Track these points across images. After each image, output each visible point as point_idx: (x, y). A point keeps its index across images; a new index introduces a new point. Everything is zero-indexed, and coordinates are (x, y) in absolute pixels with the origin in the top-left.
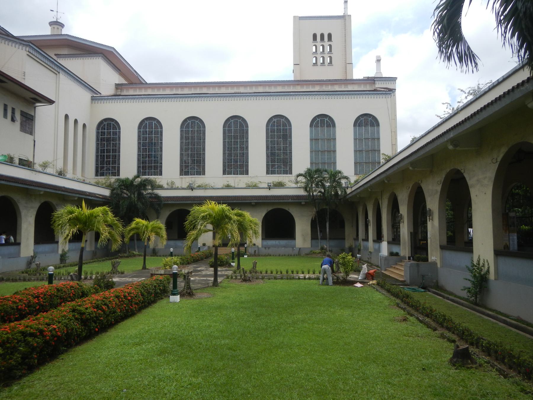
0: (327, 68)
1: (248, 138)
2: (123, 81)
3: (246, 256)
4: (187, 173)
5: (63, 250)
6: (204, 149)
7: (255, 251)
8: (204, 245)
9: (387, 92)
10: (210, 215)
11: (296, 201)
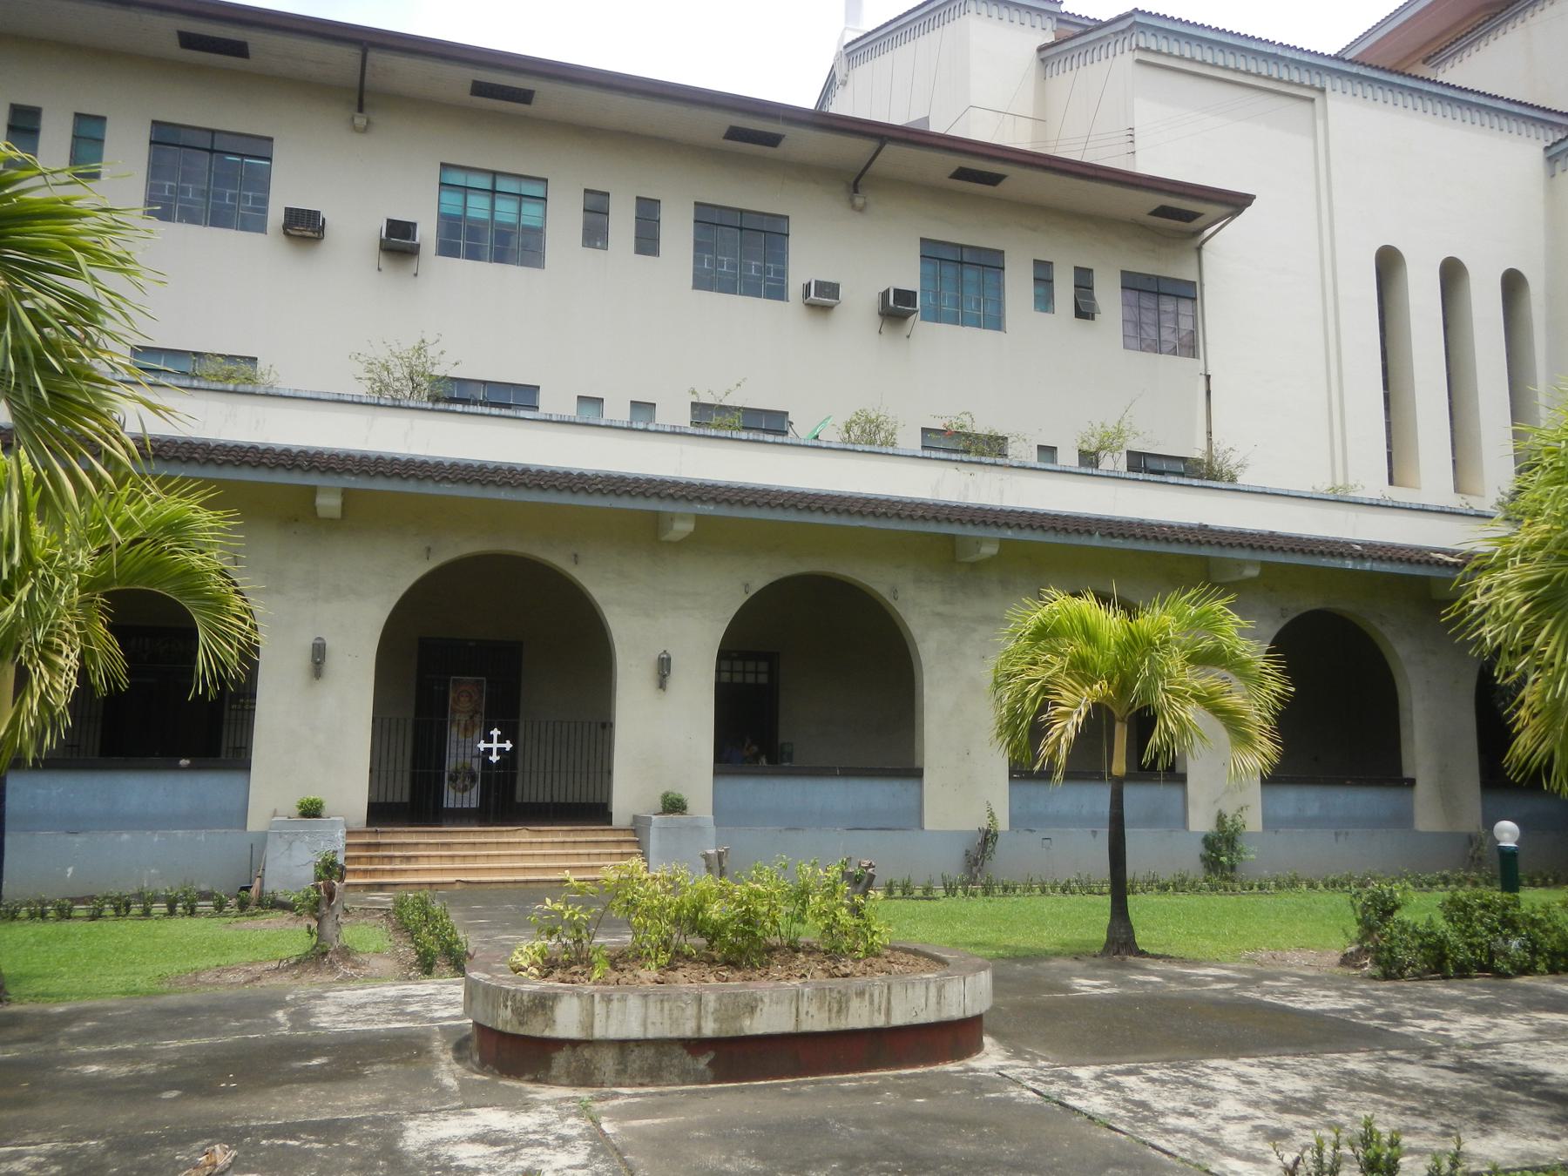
5: (1221, 819)
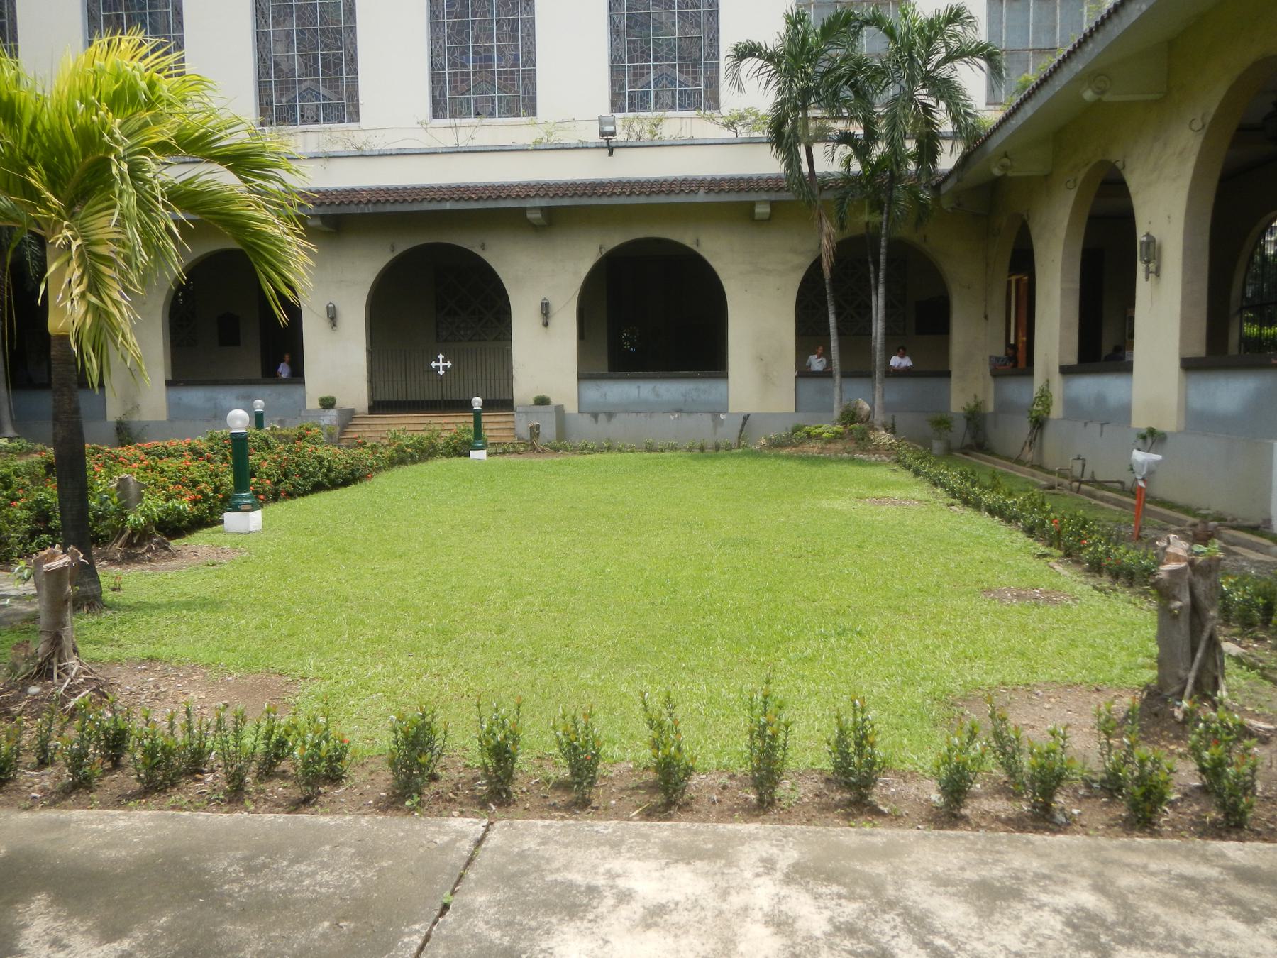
3: (478, 455)
7: (535, 431)
8: (328, 403)
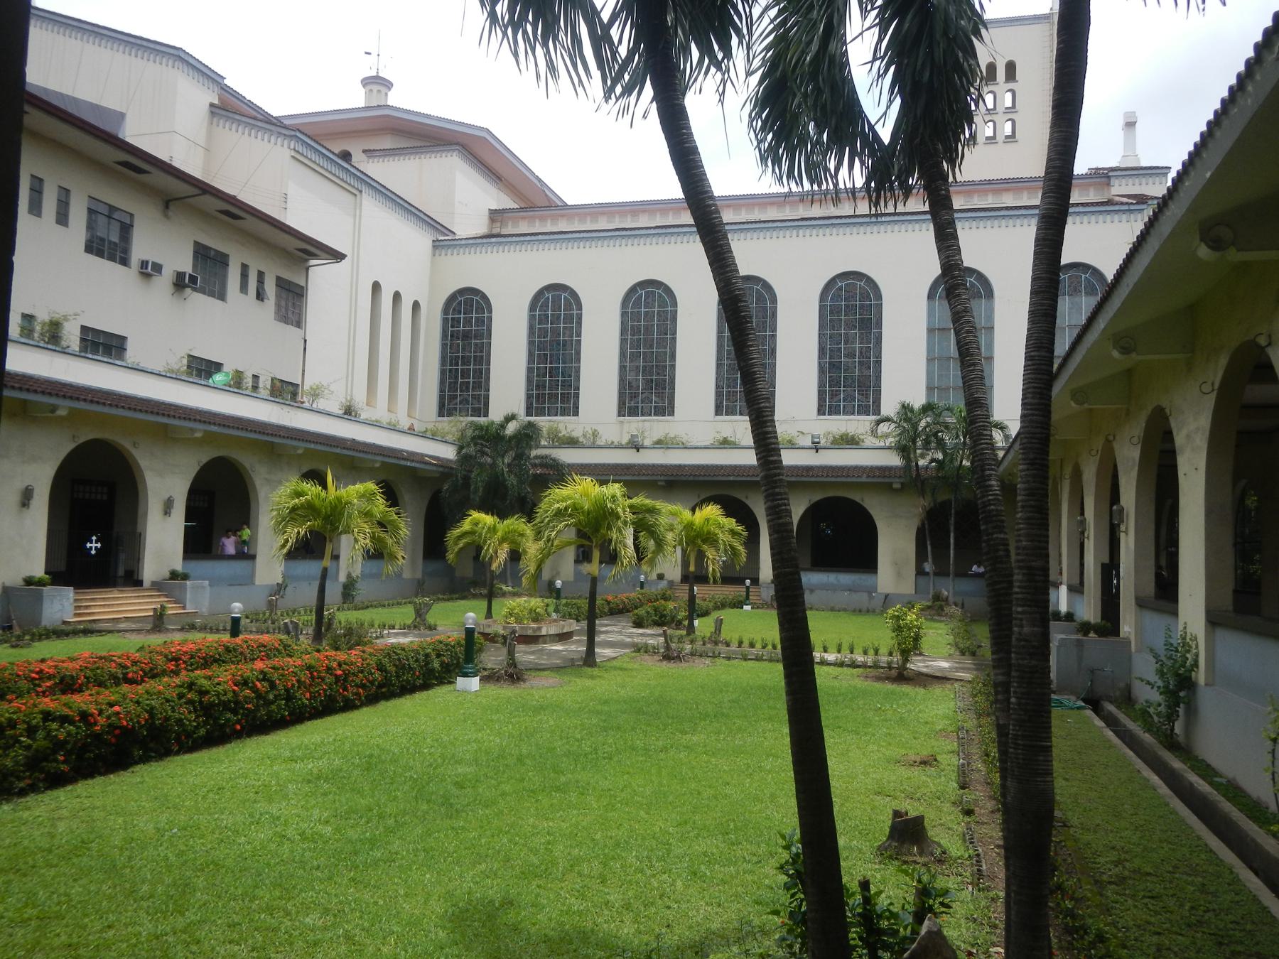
0: (1000, 149)
1: (775, 330)
2: (508, 203)
4: (633, 412)
5: (349, 576)
6: (673, 357)
9: (1132, 207)
10: (576, 507)
11: (879, 480)
